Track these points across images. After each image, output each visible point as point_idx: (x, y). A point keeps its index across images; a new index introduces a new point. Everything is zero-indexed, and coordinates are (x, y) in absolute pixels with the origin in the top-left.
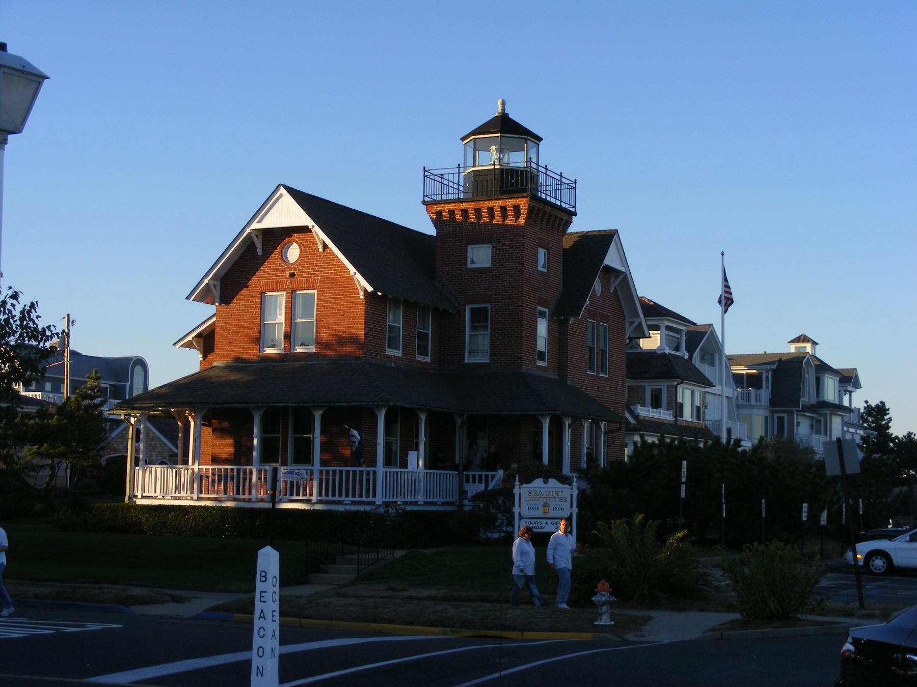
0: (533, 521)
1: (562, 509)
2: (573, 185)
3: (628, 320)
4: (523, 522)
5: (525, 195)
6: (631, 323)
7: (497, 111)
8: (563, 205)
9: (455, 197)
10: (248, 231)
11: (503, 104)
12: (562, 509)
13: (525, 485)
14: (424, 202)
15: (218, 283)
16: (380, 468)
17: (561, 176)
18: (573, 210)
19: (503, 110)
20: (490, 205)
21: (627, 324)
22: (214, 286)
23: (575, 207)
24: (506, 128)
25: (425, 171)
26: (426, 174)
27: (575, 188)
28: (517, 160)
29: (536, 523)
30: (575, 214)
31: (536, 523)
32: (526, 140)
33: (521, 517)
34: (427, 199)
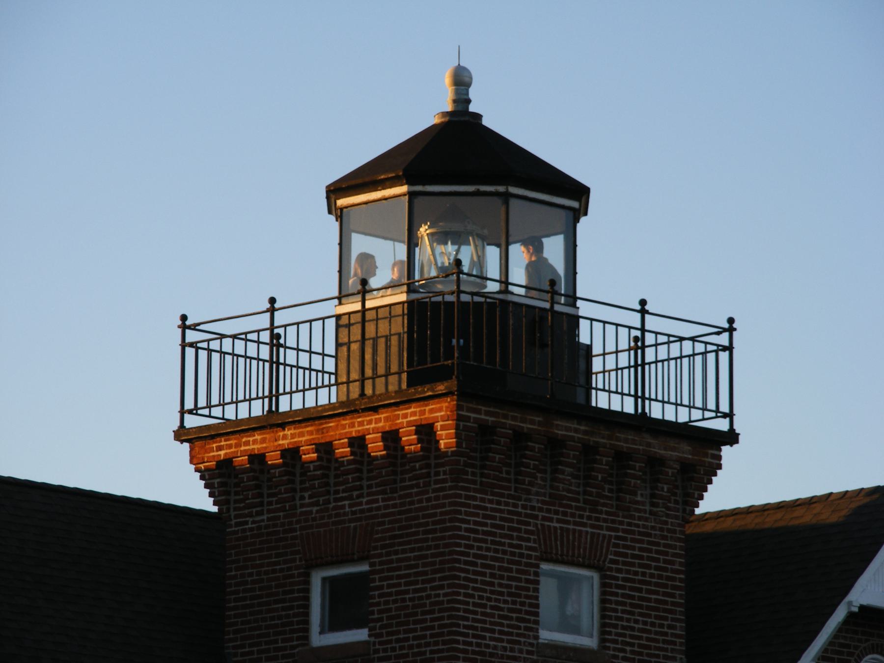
2: (724, 340)
5: (441, 388)
7: (423, 109)
8: (655, 411)
9: (258, 409)
11: (462, 81)
14: (182, 434)
17: (643, 312)
18: (722, 425)
19: (462, 100)
20: (354, 431)
23: (730, 415)
24: (461, 165)
25: (184, 327)
26: (191, 336)
27: (730, 348)
28: (507, 268)
30: (732, 437)
32: (506, 197)
34: (192, 422)
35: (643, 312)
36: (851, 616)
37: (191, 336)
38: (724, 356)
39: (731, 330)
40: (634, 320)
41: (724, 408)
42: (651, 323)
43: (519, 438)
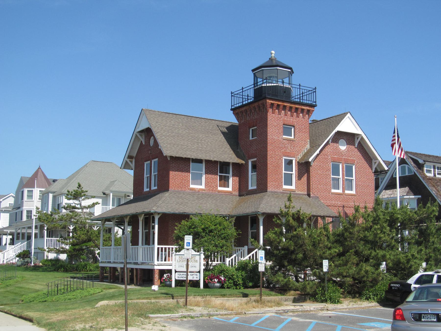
0: (182, 273)
1: (195, 267)
2: (314, 90)
3: (373, 161)
4: (177, 273)
6: (375, 163)
10: (135, 133)
12: (195, 267)
13: (177, 253)
14: (232, 110)
15: (134, 160)
16: (156, 246)
17: (300, 86)
18: (315, 103)
21: (373, 164)
22: (131, 162)
23: (315, 102)
25: (232, 93)
26: (233, 95)
27: (315, 92)
29: (183, 275)
30: (315, 106)
31: (183, 275)
33: (176, 272)
34: (233, 107)
35: (300, 86)
36: (336, 133)
37: (233, 95)
38: (314, 93)
39: (315, 89)
40: (298, 87)
41: (315, 101)
42: (301, 87)
43: (278, 105)
